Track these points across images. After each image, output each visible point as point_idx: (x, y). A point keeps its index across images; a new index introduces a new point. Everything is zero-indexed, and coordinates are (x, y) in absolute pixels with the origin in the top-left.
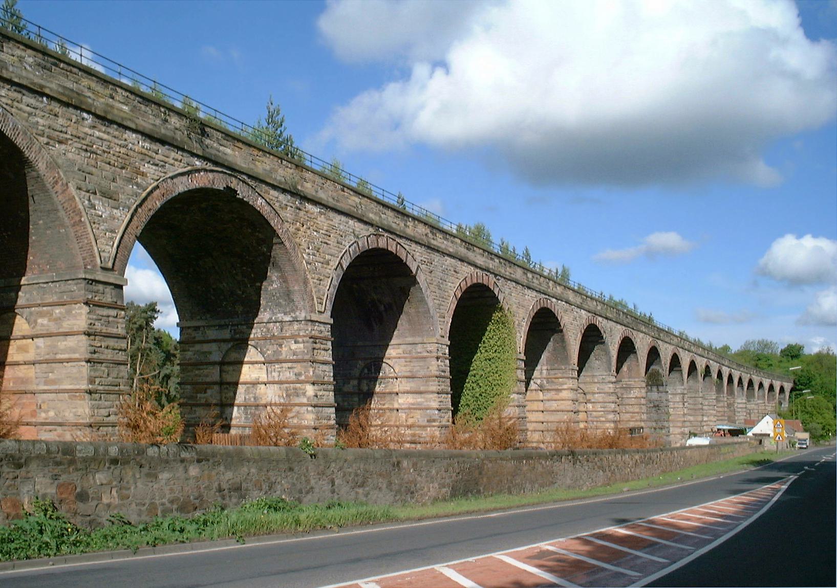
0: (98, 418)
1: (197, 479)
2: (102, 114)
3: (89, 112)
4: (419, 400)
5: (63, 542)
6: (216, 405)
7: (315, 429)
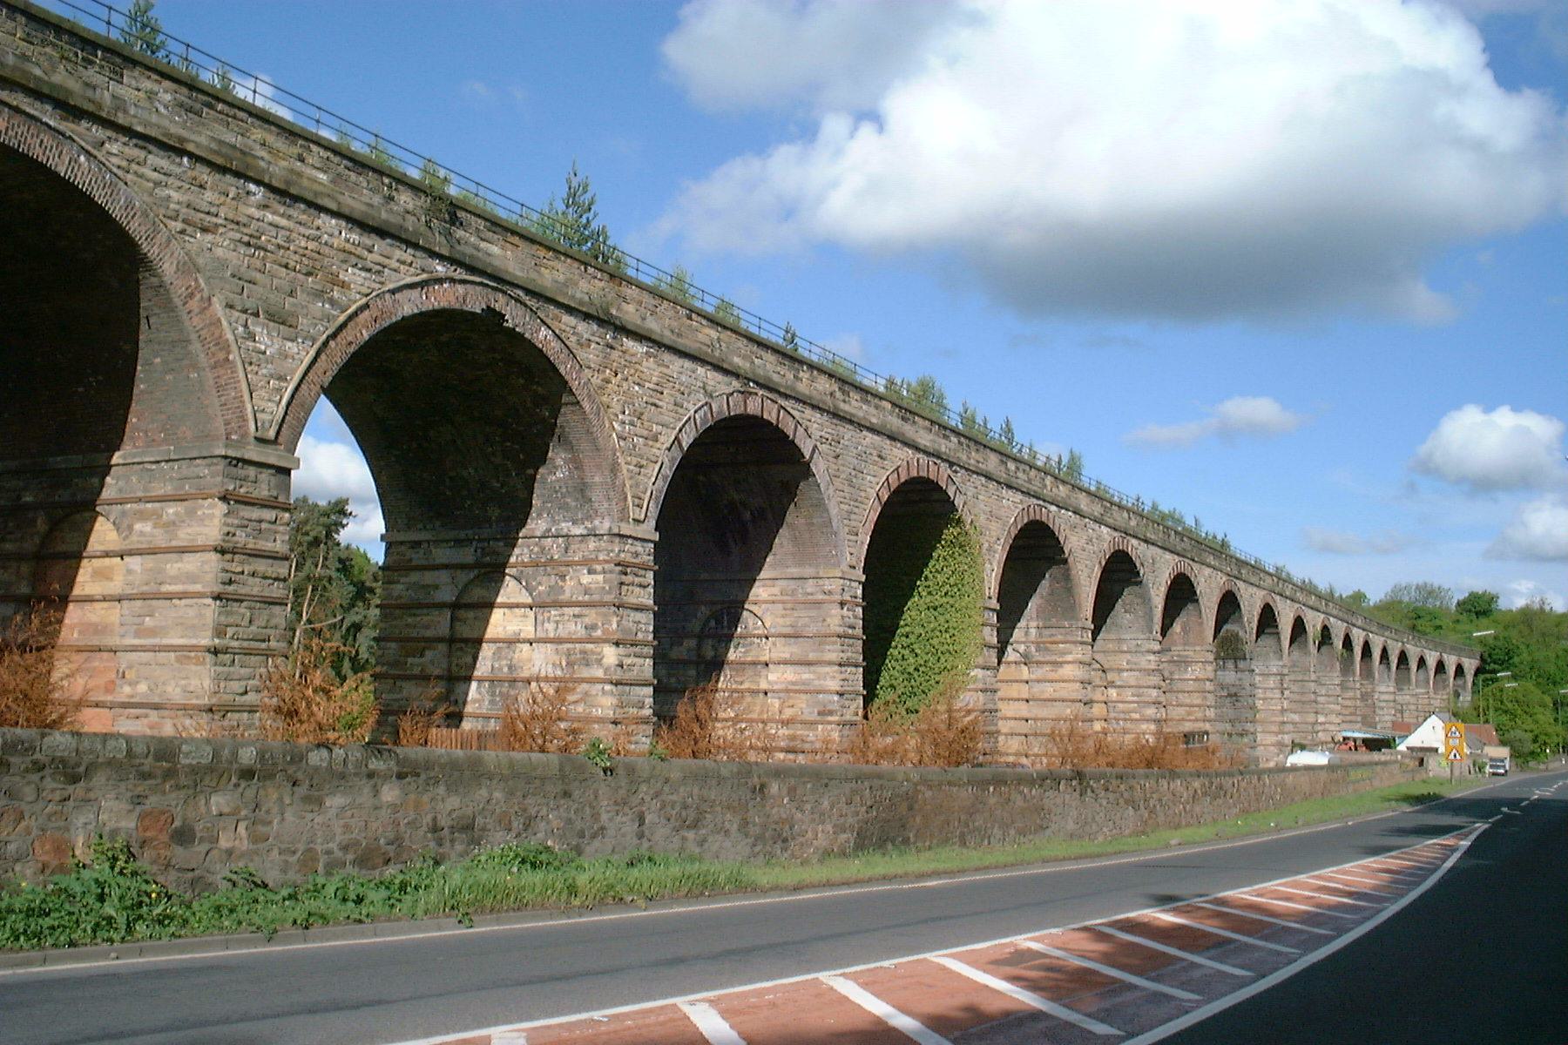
0: (226, 697)
1: (395, 808)
2: (282, 186)
3: (258, 183)
4: (805, 676)
5: (141, 917)
6: (438, 677)
7: (615, 723)
